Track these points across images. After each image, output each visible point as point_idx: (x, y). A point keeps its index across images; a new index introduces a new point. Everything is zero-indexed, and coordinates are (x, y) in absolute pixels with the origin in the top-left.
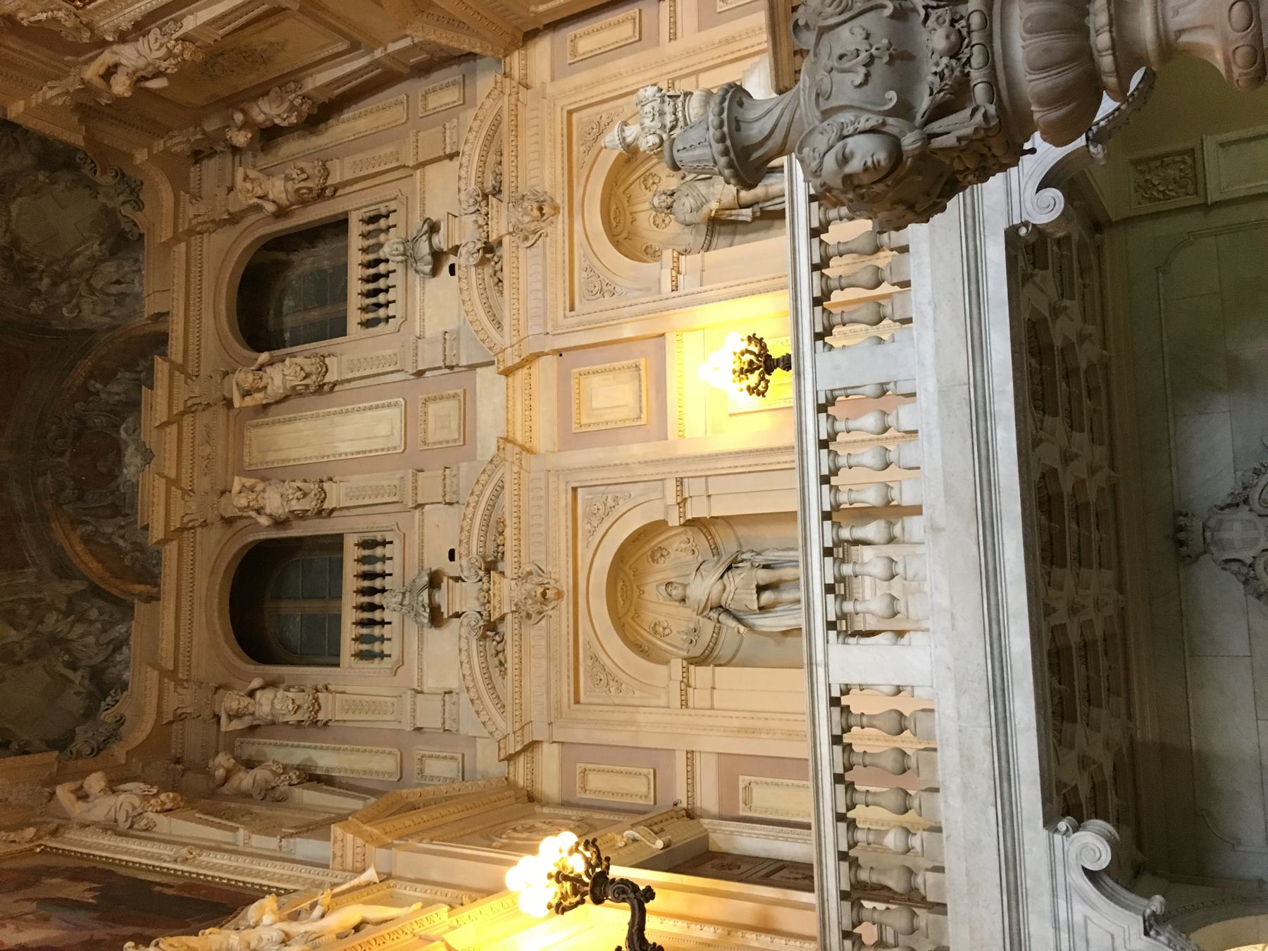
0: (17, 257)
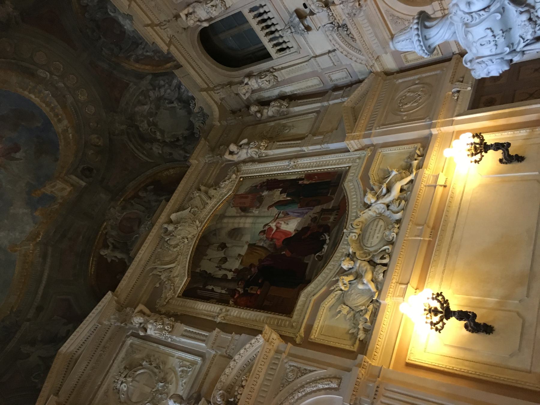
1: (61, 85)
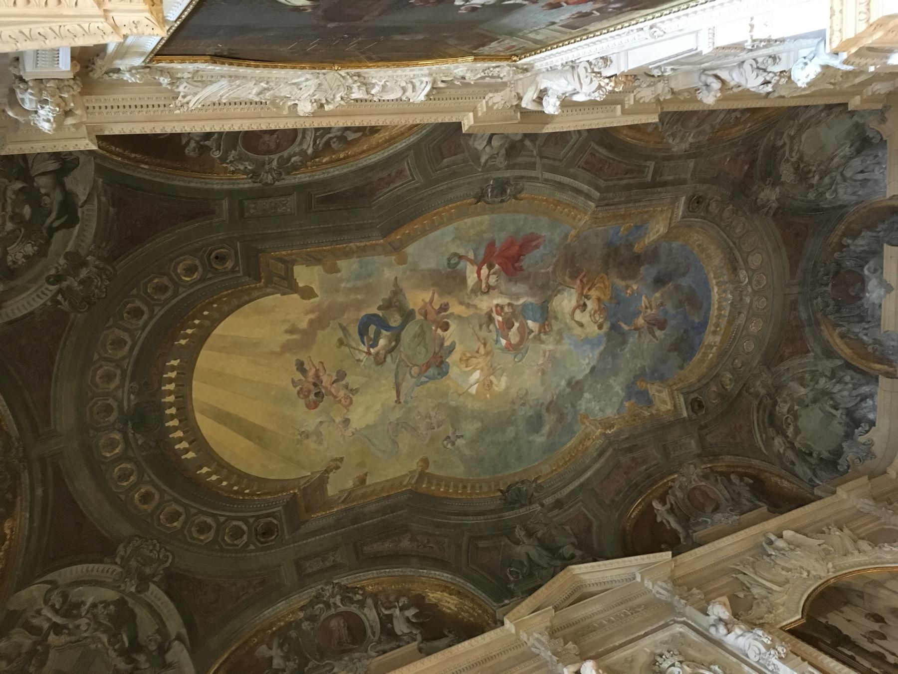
0: (802, 166)
1: (748, 300)
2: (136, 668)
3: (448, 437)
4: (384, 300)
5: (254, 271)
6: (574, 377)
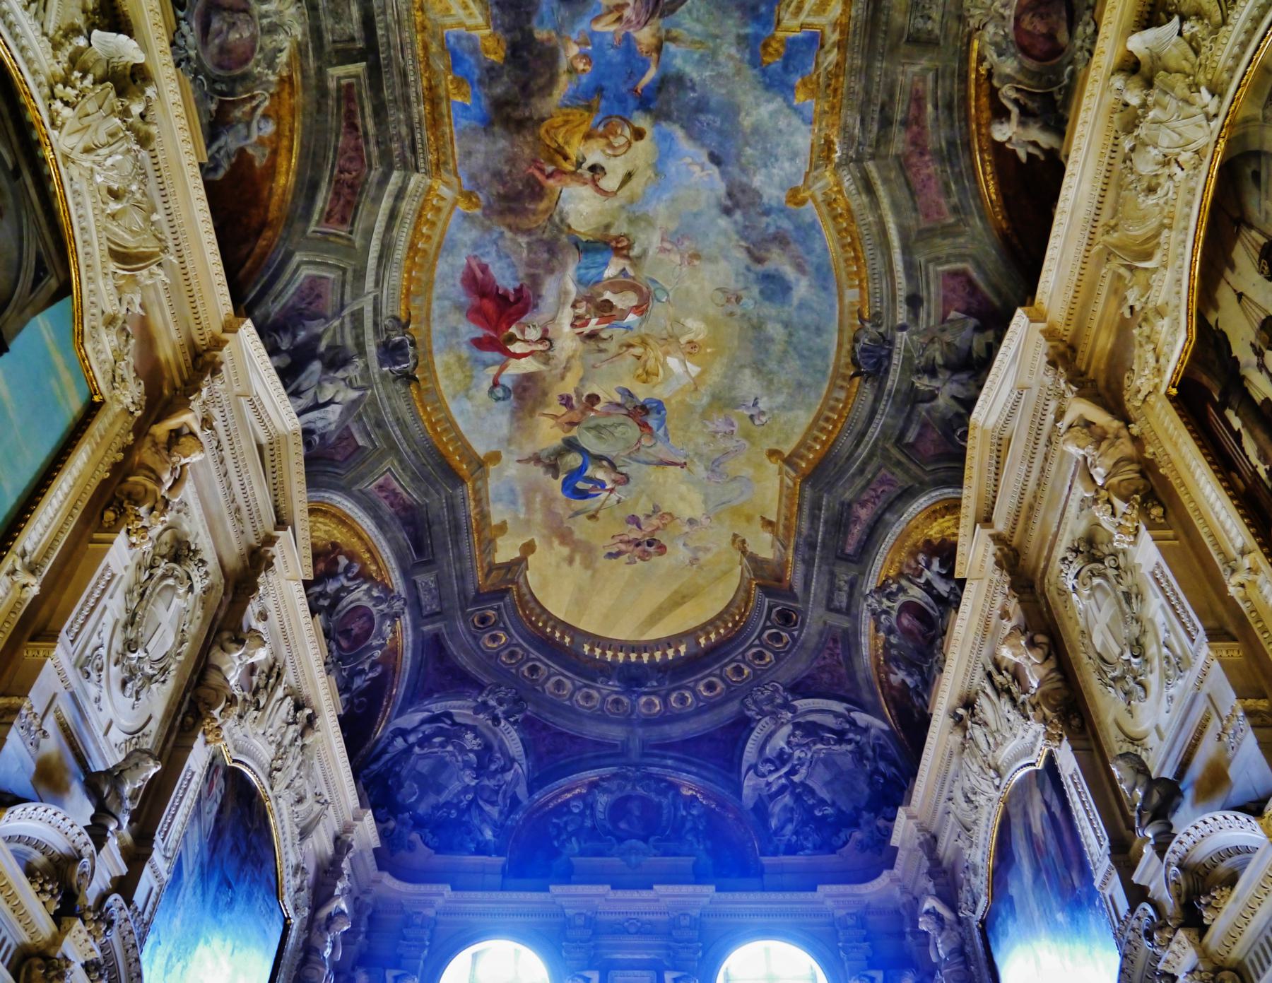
2: (857, 743)
3: (752, 417)
4: (546, 473)
5: (500, 594)
6: (718, 199)
